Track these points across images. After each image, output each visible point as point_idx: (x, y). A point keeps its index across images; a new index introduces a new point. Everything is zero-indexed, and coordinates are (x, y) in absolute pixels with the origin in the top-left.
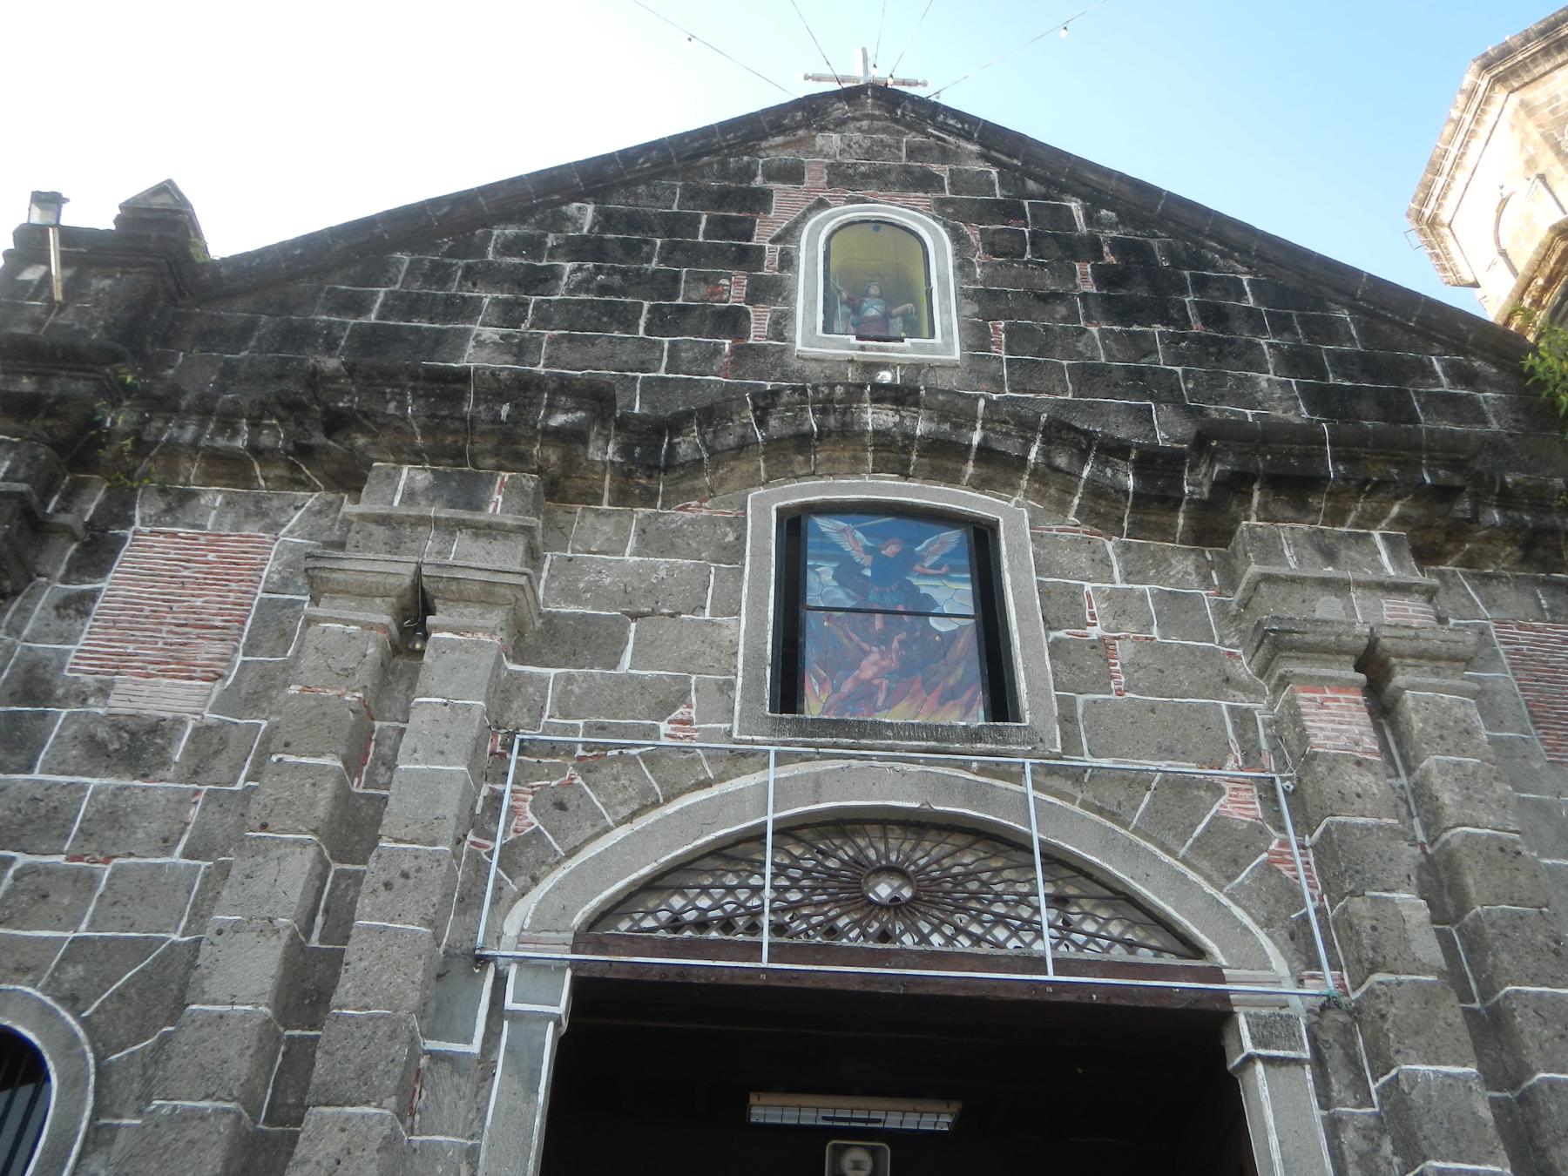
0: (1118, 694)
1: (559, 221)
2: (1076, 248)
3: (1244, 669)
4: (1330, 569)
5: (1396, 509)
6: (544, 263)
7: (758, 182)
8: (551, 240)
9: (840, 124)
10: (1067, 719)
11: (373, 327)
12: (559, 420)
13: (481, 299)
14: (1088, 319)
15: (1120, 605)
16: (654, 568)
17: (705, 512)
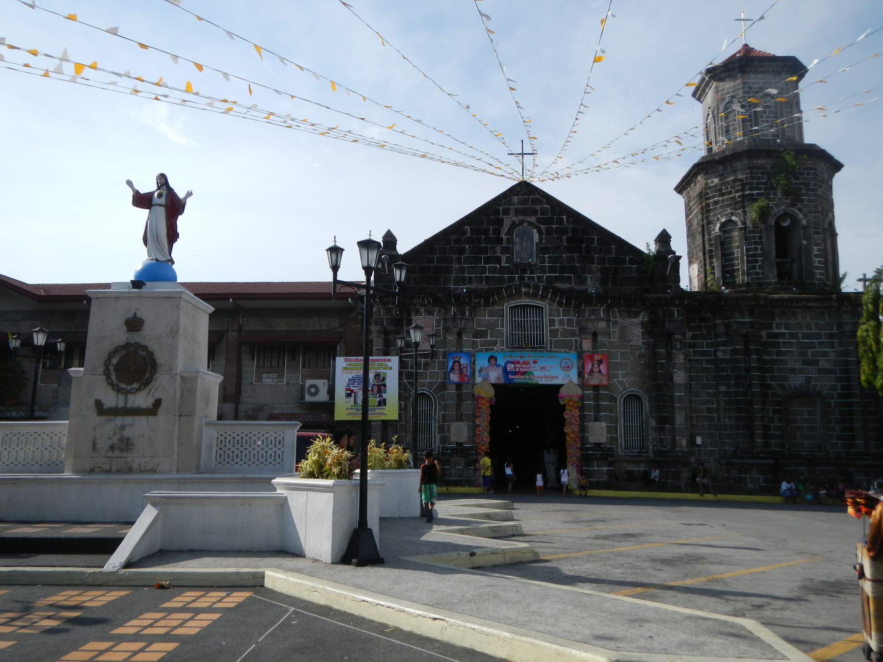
0: (559, 338)
1: (464, 233)
2: (562, 231)
3: (578, 333)
4: (592, 317)
5: (605, 305)
6: (463, 246)
7: (501, 216)
8: (463, 239)
9: (516, 195)
10: (551, 343)
11: (436, 266)
12: (476, 301)
13: (453, 257)
14: (564, 254)
15: (561, 322)
16: (491, 320)
17: (497, 308)
